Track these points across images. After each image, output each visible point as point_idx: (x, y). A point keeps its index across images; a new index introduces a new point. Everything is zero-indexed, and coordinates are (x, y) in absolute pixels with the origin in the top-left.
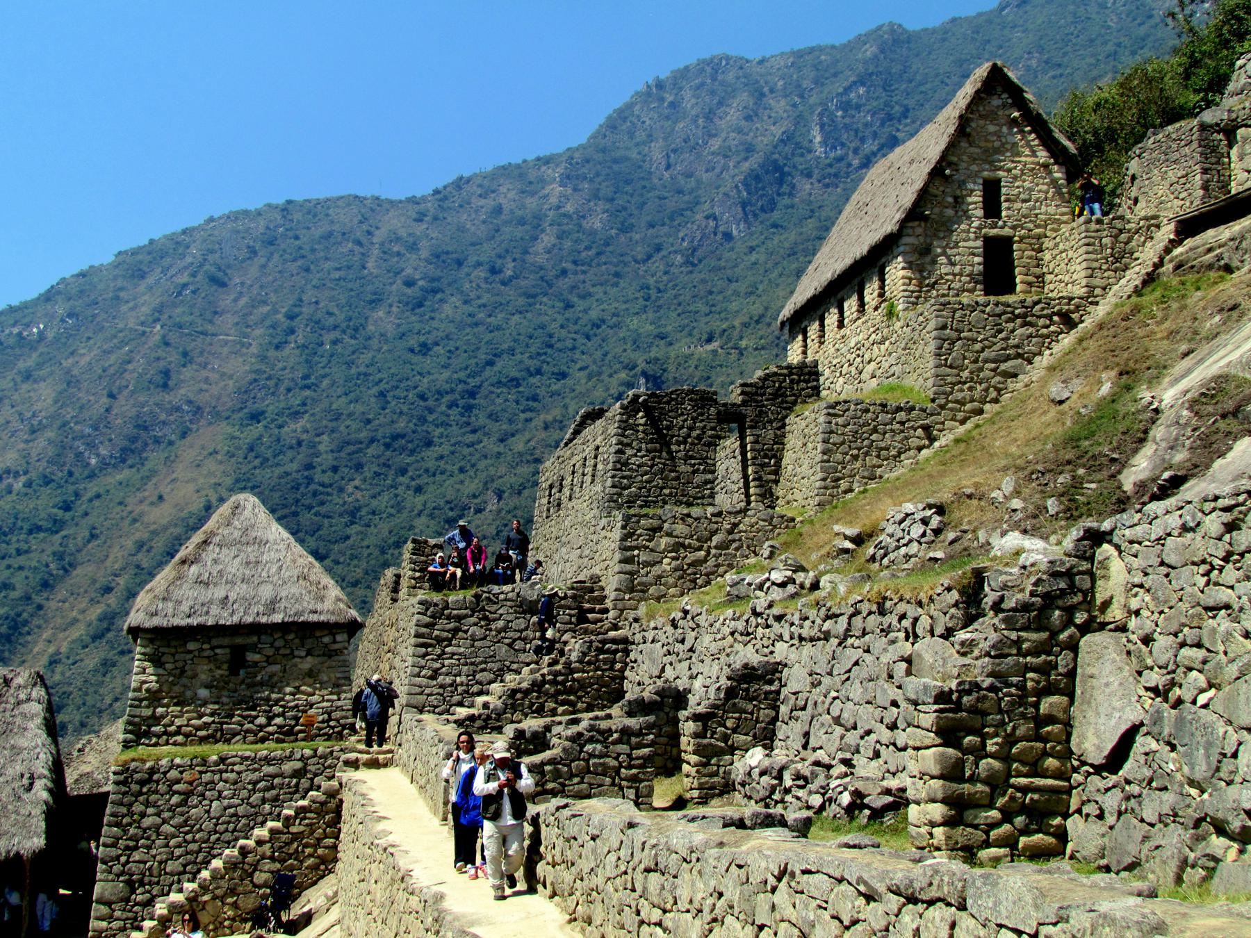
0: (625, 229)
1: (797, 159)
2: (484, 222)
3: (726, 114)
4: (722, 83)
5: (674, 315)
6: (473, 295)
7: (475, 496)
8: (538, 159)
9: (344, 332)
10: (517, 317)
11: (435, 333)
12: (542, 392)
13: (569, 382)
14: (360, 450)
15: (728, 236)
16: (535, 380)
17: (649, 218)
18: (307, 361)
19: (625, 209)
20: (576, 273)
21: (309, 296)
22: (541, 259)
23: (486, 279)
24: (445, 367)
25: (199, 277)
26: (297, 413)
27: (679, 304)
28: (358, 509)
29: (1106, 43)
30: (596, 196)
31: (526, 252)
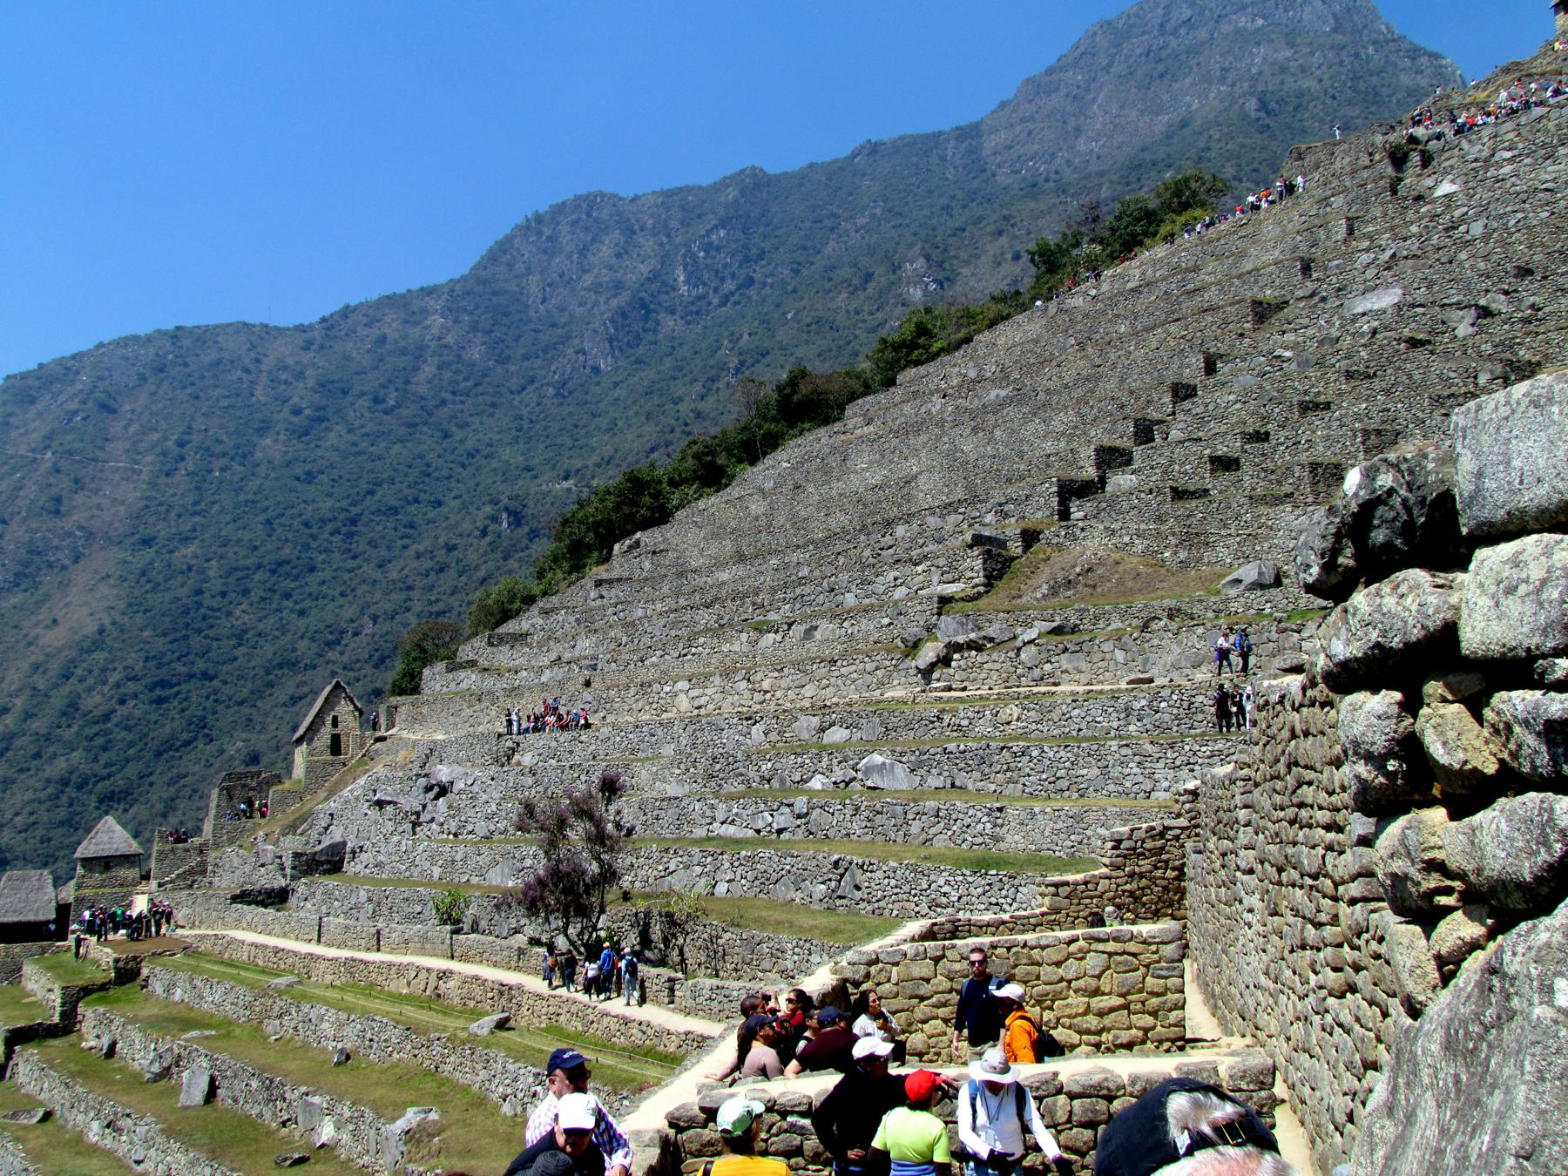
0: (502, 360)
1: (663, 297)
2: (369, 351)
3: (599, 250)
4: (596, 221)
5: (541, 447)
6: (356, 424)
7: (352, 621)
8: (422, 289)
9: (232, 459)
10: (397, 447)
11: (320, 462)
12: (418, 521)
13: (444, 509)
14: (248, 576)
15: (596, 370)
16: (412, 508)
18: (198, 488)
20: (454, 403)
21: (199, 424)
24: (329, 495)
25: (90, 404)
26: (187, 538)
28: (245, 631)
29: (941, 195)
30: (474, 328)
31: (408, 382)
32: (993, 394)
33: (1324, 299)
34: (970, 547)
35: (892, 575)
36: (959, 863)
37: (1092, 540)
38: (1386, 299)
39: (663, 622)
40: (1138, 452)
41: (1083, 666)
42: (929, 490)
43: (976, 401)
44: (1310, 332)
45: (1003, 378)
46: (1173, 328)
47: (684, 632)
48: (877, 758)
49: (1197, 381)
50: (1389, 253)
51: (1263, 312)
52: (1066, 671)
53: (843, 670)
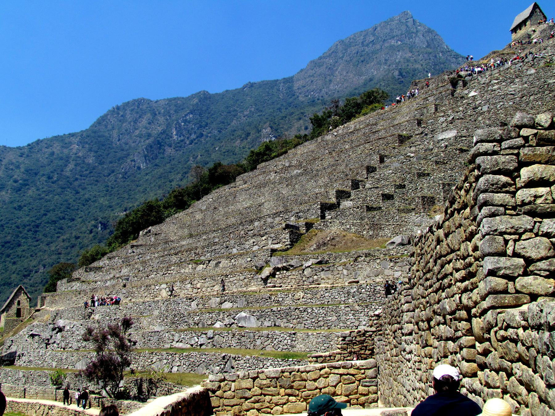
5: (116, 198)
8: (70, 134)
15: (139, 168)
17: (110, 160)
19: (102, 156)
22: (68, 174)
23: (46, 181)
27: (118, 194)
30: (90, 150)
32: (295, 172)
33: (426, 135)
34: (284, 229)
35: (252, 241)
36: (276, 356)
37: (334, 228)
38: (451, 134)
39: (157, 261)
40: (353, 193)
41: (330, 276)
42: (268, 207)
43: (288, 174)
44: (421, 147)
45: (300, 165)
46: (367, 146)
47: (166, 265)
48: (243, 314)
49: (376, 166)
50: (451, 117)
51: (402, 139)
52: (323, 279)
53: (231, 279)
